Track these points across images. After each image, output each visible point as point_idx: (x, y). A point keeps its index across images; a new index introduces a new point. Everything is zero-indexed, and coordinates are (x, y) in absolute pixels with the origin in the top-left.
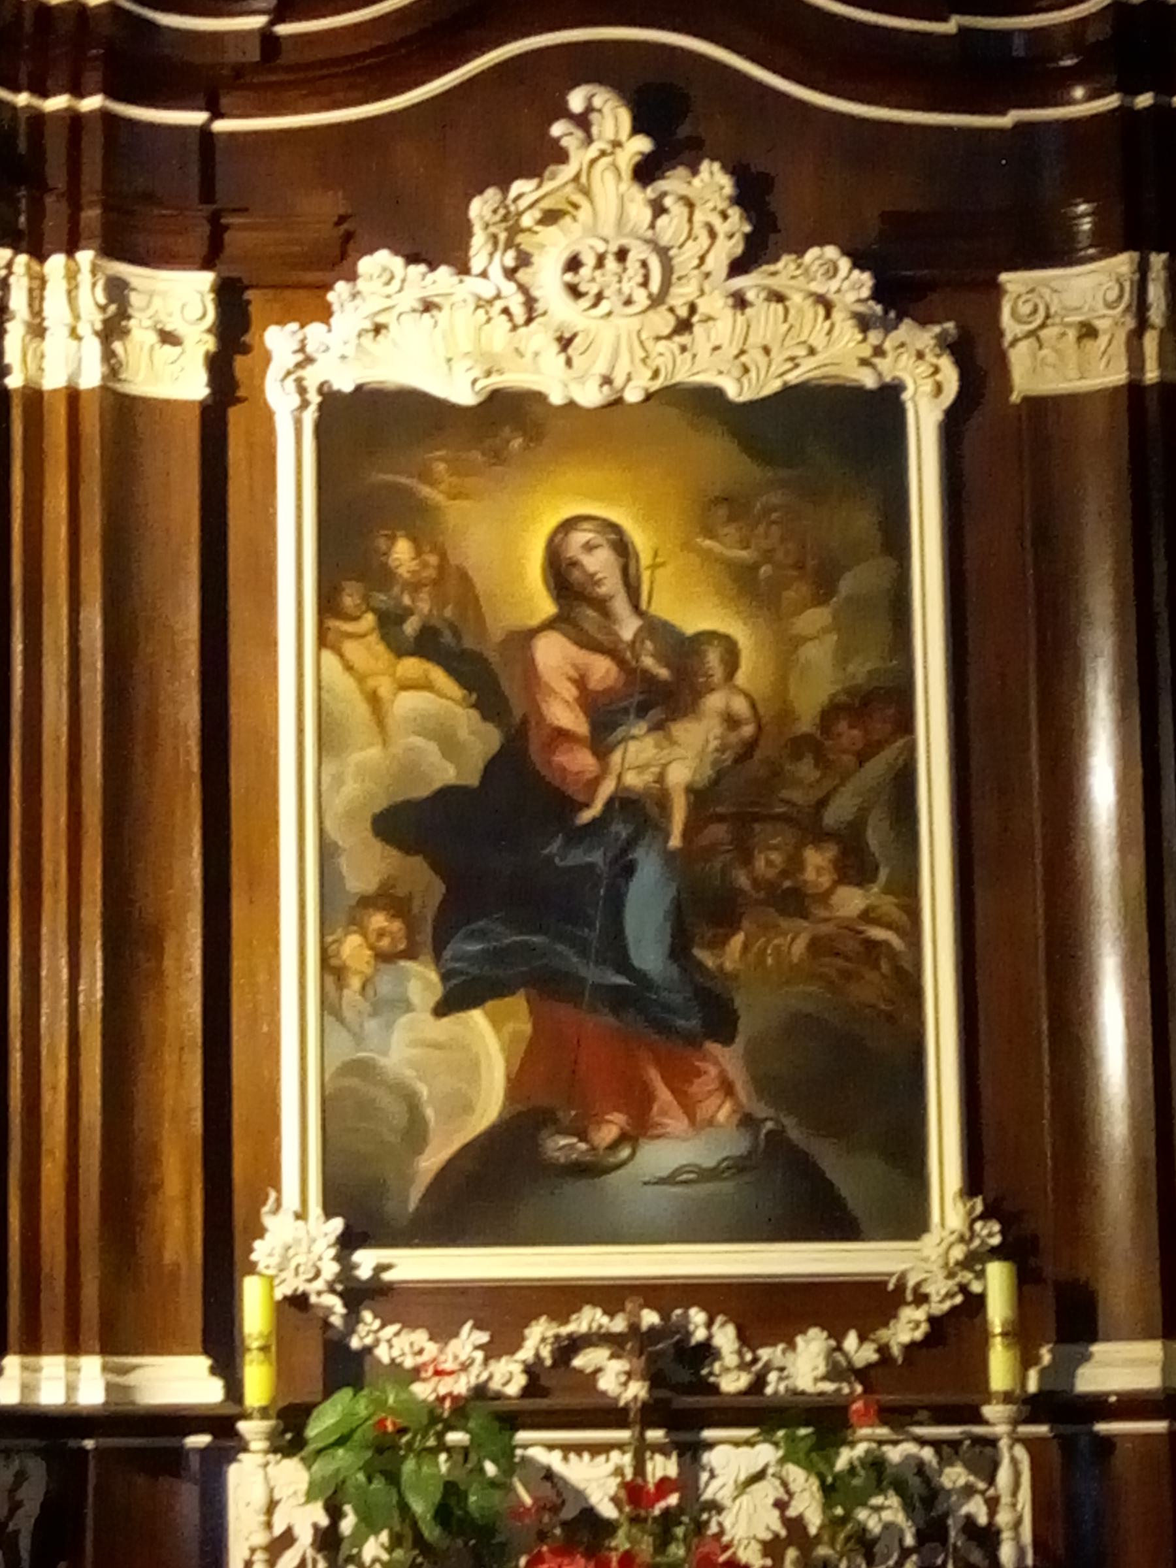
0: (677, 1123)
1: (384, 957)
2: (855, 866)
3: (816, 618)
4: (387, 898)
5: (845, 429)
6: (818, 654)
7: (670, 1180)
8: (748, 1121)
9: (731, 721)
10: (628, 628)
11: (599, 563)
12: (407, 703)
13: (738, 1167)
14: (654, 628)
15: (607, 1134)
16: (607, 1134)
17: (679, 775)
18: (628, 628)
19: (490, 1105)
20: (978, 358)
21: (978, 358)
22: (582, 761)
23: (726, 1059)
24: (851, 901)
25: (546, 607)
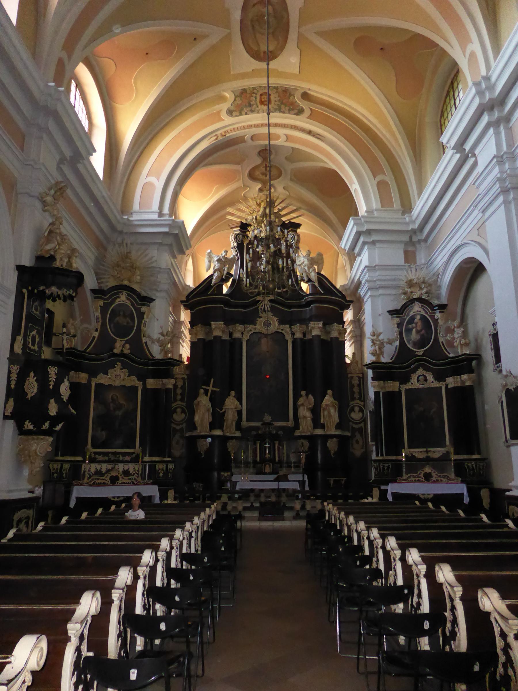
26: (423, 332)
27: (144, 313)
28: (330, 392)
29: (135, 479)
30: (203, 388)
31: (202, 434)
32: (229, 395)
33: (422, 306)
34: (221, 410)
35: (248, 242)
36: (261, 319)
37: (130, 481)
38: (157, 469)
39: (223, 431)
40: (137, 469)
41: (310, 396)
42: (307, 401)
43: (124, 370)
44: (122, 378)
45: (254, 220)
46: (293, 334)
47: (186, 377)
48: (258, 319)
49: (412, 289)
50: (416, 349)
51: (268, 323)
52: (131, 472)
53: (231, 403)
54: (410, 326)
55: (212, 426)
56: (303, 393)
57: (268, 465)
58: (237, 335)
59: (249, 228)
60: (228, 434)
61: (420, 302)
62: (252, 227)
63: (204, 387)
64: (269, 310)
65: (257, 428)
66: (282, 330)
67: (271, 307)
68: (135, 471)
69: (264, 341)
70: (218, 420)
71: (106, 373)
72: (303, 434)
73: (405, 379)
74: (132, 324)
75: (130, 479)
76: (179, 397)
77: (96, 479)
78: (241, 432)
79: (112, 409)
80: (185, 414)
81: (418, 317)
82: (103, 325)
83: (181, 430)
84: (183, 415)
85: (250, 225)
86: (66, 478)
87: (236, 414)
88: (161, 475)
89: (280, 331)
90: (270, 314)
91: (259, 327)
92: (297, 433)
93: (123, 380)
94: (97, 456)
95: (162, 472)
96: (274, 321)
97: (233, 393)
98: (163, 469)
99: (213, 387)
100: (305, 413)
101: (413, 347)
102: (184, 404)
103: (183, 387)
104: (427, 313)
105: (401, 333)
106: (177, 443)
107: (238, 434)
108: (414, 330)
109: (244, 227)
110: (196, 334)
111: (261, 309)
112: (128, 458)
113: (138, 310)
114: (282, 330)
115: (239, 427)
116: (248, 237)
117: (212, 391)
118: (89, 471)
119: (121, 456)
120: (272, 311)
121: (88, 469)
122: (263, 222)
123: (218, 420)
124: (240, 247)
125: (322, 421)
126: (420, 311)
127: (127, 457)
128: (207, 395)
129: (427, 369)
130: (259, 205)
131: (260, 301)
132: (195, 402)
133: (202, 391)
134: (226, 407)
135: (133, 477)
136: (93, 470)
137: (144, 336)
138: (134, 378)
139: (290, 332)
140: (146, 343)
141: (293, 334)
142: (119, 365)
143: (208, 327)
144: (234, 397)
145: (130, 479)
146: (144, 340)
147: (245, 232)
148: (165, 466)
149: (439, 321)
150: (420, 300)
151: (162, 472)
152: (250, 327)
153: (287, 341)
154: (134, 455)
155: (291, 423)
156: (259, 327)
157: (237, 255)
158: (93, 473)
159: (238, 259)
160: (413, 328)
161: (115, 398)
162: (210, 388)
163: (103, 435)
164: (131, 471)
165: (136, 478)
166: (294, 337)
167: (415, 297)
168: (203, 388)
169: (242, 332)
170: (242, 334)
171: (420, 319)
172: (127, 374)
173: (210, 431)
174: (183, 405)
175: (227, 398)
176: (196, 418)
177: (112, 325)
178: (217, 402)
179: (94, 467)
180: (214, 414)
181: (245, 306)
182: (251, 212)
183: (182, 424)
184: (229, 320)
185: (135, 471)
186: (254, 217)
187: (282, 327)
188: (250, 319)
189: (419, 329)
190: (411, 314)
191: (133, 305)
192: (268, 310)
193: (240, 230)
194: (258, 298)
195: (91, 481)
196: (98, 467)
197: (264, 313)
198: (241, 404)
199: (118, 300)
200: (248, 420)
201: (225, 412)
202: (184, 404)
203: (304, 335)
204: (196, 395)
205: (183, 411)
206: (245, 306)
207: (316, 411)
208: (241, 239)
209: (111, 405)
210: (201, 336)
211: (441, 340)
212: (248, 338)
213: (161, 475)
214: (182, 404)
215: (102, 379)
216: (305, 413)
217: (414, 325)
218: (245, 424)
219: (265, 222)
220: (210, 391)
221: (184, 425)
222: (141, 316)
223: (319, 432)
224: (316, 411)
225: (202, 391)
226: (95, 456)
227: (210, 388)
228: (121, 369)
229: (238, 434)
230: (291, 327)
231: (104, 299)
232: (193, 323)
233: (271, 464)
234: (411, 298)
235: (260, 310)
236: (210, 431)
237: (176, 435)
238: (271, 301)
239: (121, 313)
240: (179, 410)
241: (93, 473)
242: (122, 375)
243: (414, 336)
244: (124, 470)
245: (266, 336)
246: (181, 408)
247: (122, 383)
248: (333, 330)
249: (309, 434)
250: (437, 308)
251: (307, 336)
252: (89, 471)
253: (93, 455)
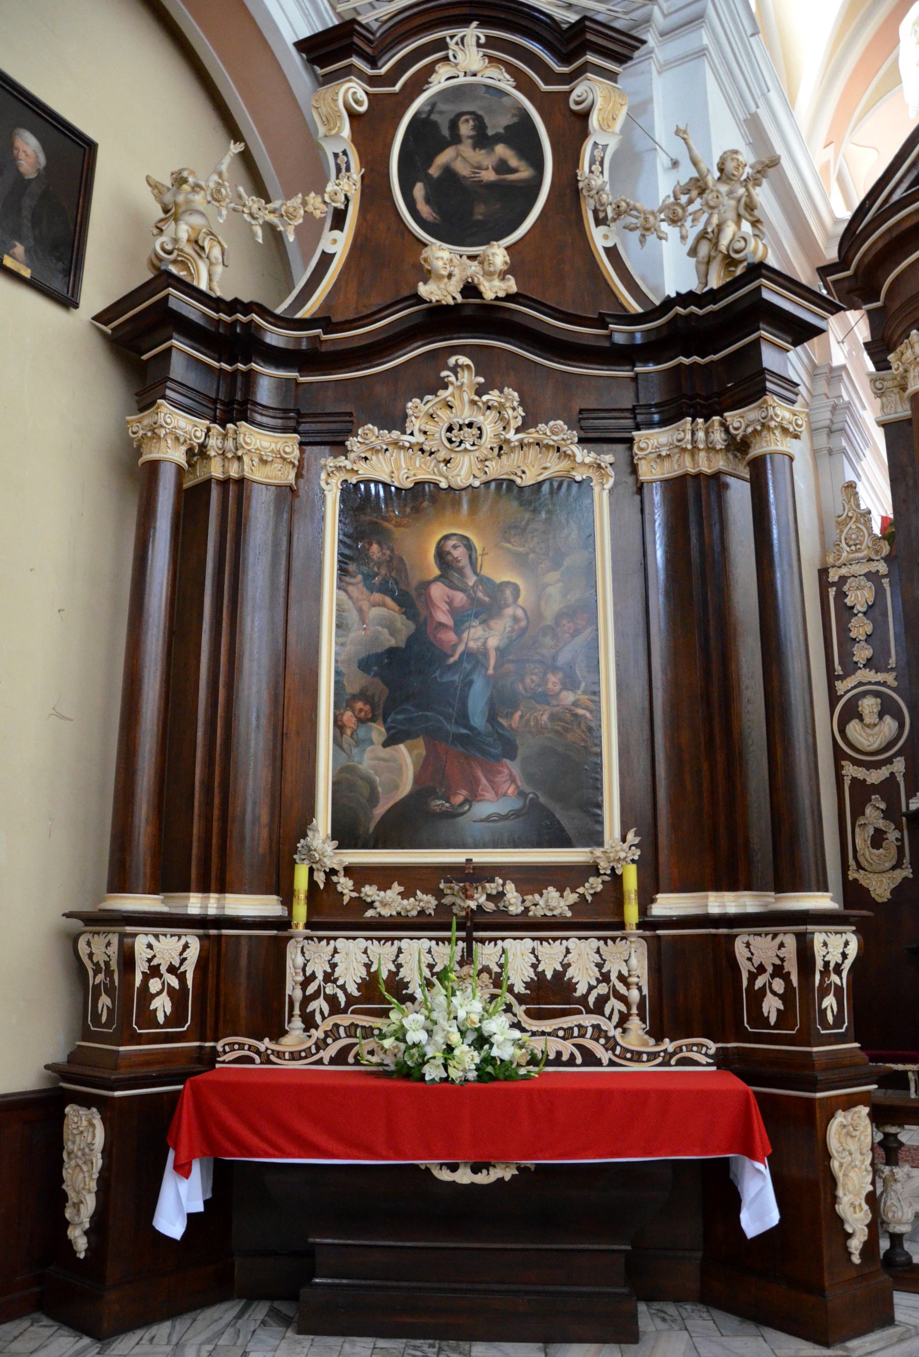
0: (490, 795)
1: (361, 721)
4: (363, 695)
7: (487, 819)
13: (516, 814)
15: (459, 799)
16: (459, 799)
19: (406, 786)
23: (513, 767)
27: (584, 116)
29: (598, 1032)
37: (568, 1048)
38: (745, 968)
40: (614, 967)
43: (493, 396)
44: (489, 439)
47: (883, 568)
52: (581, 990)
68: (605, 978)
71: (395, 421)
74: (525, 173)
75: (568, 1034)
76: (862, 653)
77: (351, 1030)
79: (442, 616)
80: (898, 716)
82: (374, 188)
83: (888, 788)
84: (889, 725)
86: (170, 1021)
88: (771, 1006)
93: (501, 448)
94: (370, 892)
95: (779, 985)
98: (779, 971)
102: (890, 678)
103: (873, 610)
106: (878, 840)
112: (555, 902)
113: (554, 107)
118: (329, 978)
119: (510, 887)
121: (319, 968)
127: (552, 893)
135: (587, 1020)
136: (351, 975)
137: (599, 222)
138: (556, 431)
140: (612, 252)
142: (463, 378)
145: (568, 1034)
146: (599, 238)
148: (790, 942)
151: (779, 985)
154: (595, 884)
158: (353, 990)
161: (459, 553)
163: (398, 769)
164: (582, 976)
165: (608, 1026)
172: (515, 416)
174: (884, 684)
177: (419, 191)
179: (352, 958)
183: (889, 761)
185: (605, 978)
191: (523, 84)
195: (321, 1045)
196: (383, 956)
199: (443, 71)
202: (890, 678)
205: (887, 708)
209: (438, 591)
213: (771, 1006)
214: (880, 677)
215: (381, 460)
221: (899, 766)
222: (573, 126)
226: (357, 888)
228: (481, 391)
231: (372, 81)
237: (868, 810)
239: (466, 129)
240: (869, 706)
241: (353, 990)
242: (489, 423)
244: (541, 975)
246: (877, 694)
247: (495, 469)
252: (329, 978)
253: (345, 885)
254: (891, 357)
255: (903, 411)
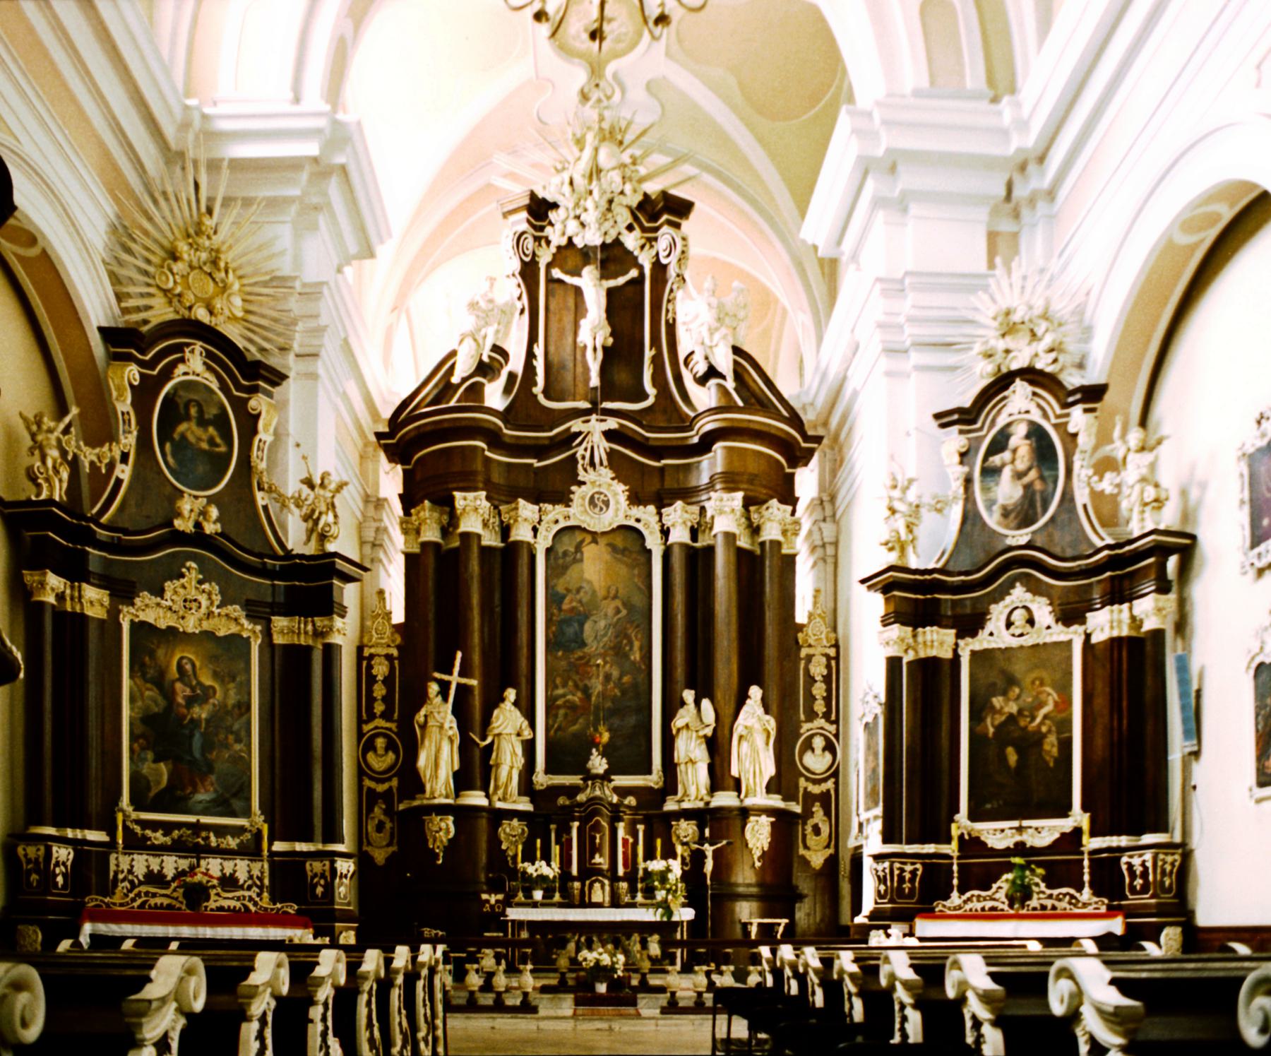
2: (238, 740)
3: (231, 685)
5: (236, 644)
6: (232, 693)
8: (216, 791)
9: (214, 705)
10: (194, 683)
11: (188, 667)
12: (147, 693)
14: (200, 684)
17: (204, 716)
18: (194, 683)
20: (268, 633)
21: (268, 633)
22: (185, 711)
24: (237, 747)
25: (177, 676)
26: (1033, 474)
28: (755, 692)
30: (437, 680)
31: (436, 801)
32: (503, 700)
33: (1034, 394)
34: (484, 739)
35: (549, 258)
36: (583, 487)
39: (487, 796)
41: (706, 704)
42: (696, 718)
45: (567, 189)
46: (665, 532)
48: (574, 488)
49: (1008, 342)
50: (1007, 527)
51: (600, 500)
53: (507, 719)
54: (996, 460)
55: (462, 781)
56: (689, 695)
57: (597, 885)
58: (521, 533)
59: (552, 215)
60: (499, 805)
61: (1032, 383)
62: (561, 211)
63: (437, 675)
64: (605, 463)
65: (572, 791)
66: (638, 520)
67: (611, 454)
69: (590, 551)
70: (475, 767)
72: (686, 805)
73: (970, 624)
78: (532, 802)
81: (1020, 430)
85: (555, 206)
87: (519, 750)
89: (632, 523)
90: (606, 474)
91: (577, 512)
92: (670, 805)
96: (616, 494)
97: (511, 694)
99: (461, 674)
100: (691, 750)
101: (999, 524)
104: (1045, 416)
105: (968, 481)
107: (525, 805)
108: (1007, 473)
109: (539, 209)
110: (418, 532)
111: (583, 458)
114: (638, 520)
115: (526, 787)
116: (548, 243)
117: (459, 685)
120: (611, 466)
122: (591, 193)
123: (475, 767)
124: (528, 271)
125: (734, 772)
126: (1027, 412)
128: (445, 699)
129: (1035, 588)
130: (580, 142)
131: (580, 433)
132: (420, 717)
133: (434, 688)
134: (496, 731)
139: (657, 527)
141: (665, 532)
143: (447, 509)
144: (516, 704)
147: (542, 229)
149: (1080, 439)
150: (1031, 375)
152: (554, 512)
153: (650, 551)
155: (654, 779)
156: (577, 512)
157: (519, 298)
159: (522, 311)
160: (1003, 465)
162: (455, 679)
166: (667, 540)
167: (1015, 366)
168: (437, 680)
169: (533, 524)
170: (535, 530)
171: (1027, 437)
173: (457, 796)
175: (496, 706)
176: (423, 761)
178: (473, 719)
180: (466, 748)
181: (540, 450)
182: (559, 166)
184: (504, 493)
186: (567, 181)
187: (638, 511)
188: (554, 487)
189: (1021, 465)
190: (1002, 421)
192: (601, 464)
193: (528, 221)
194: (576, 425)
197: (590, 469)
198: (532, 726)
200: (549, 770)
201: (492, 743)
203: (694, 533)
204: (421, 698)
206: (540, 450)
207: (718, 747)
208: (530, 247)
210: (431, 534)
211: (1082, 497)
212: (549, 543)
216: (691, 750)
217: (1007, 455)
218: (541, 779)
219: (596, 193)
220: (453, 687)
223: (726, 799)
224: (718, 747)
225: (434, 688)
227: (455, 679)
229: (525, 805)
230: (660, 514)
232: (409, 500)
233: (606, 882)
234: (1004, 370)
235: (581, 462)
236: (457, 796)
238: (609, 435)
243: (1008, 491)
245: (594, 534)
248: (769, 520)
249: (701, 805)
250: (1078, 396)
251: (700, 537)
254: (413, 511)
255: (417, 550)
